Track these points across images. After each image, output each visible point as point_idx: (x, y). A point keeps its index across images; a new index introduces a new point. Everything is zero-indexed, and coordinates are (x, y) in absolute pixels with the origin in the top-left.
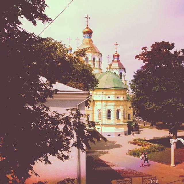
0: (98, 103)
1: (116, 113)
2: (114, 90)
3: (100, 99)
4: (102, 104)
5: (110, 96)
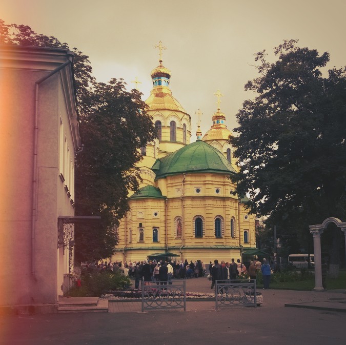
0: (177, 203)
3: (179, 194)
5: (200, 189)
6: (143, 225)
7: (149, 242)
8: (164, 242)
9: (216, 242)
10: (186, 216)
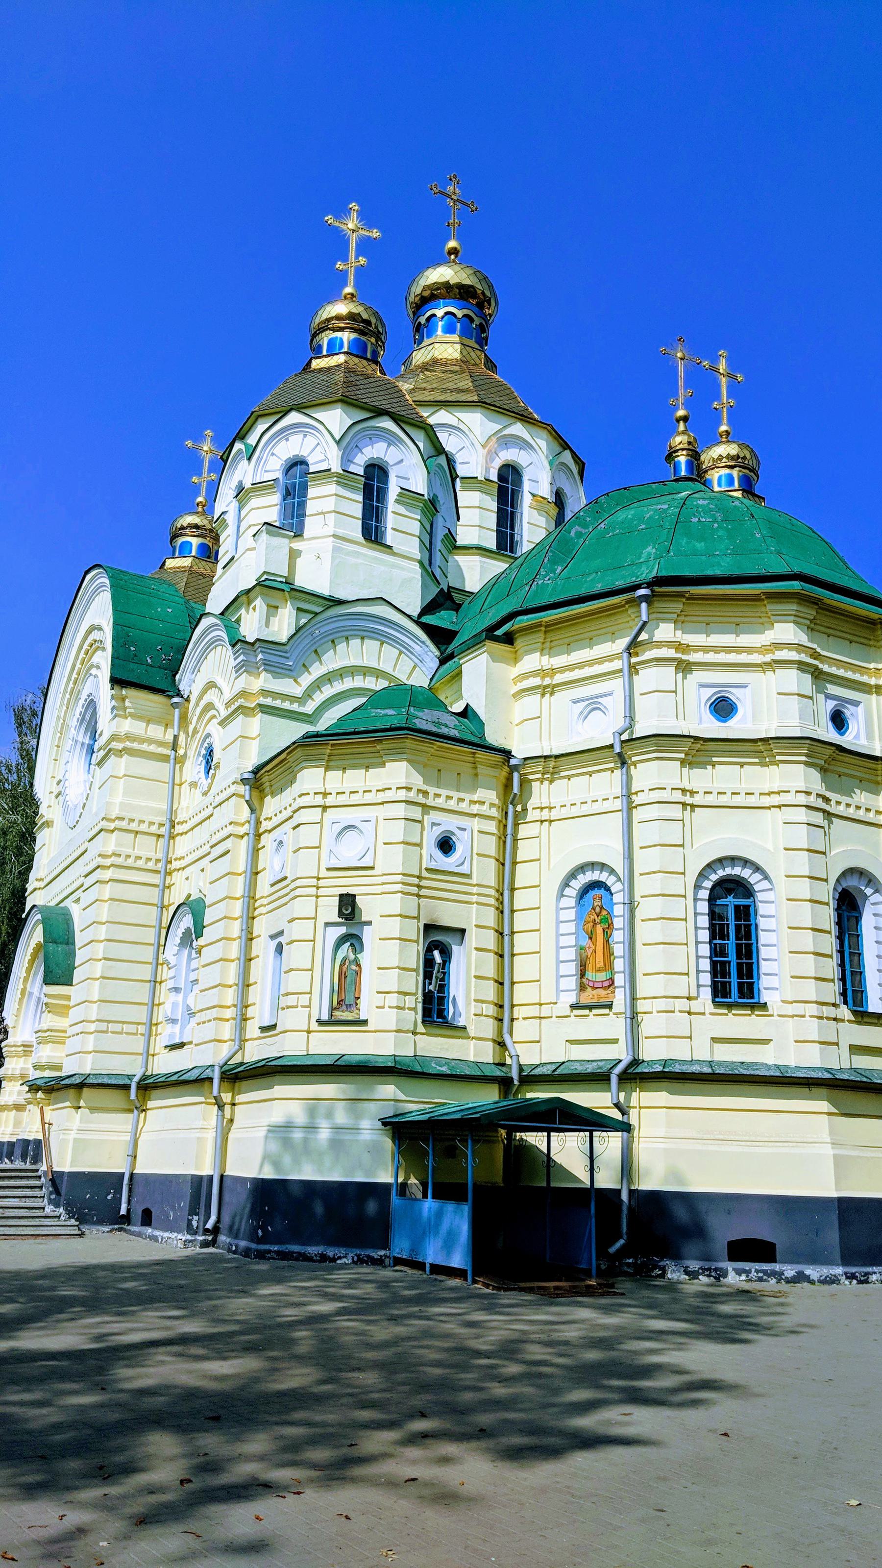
1: (827, 917)
2: (792, 607)
3: (602, 730)
4: (628, 795)
5: (735, 695)
6: (367, 907)
7: (386, 1026)
8: (488, 1028)
9: (856, 1049)
10: (643, 860)
